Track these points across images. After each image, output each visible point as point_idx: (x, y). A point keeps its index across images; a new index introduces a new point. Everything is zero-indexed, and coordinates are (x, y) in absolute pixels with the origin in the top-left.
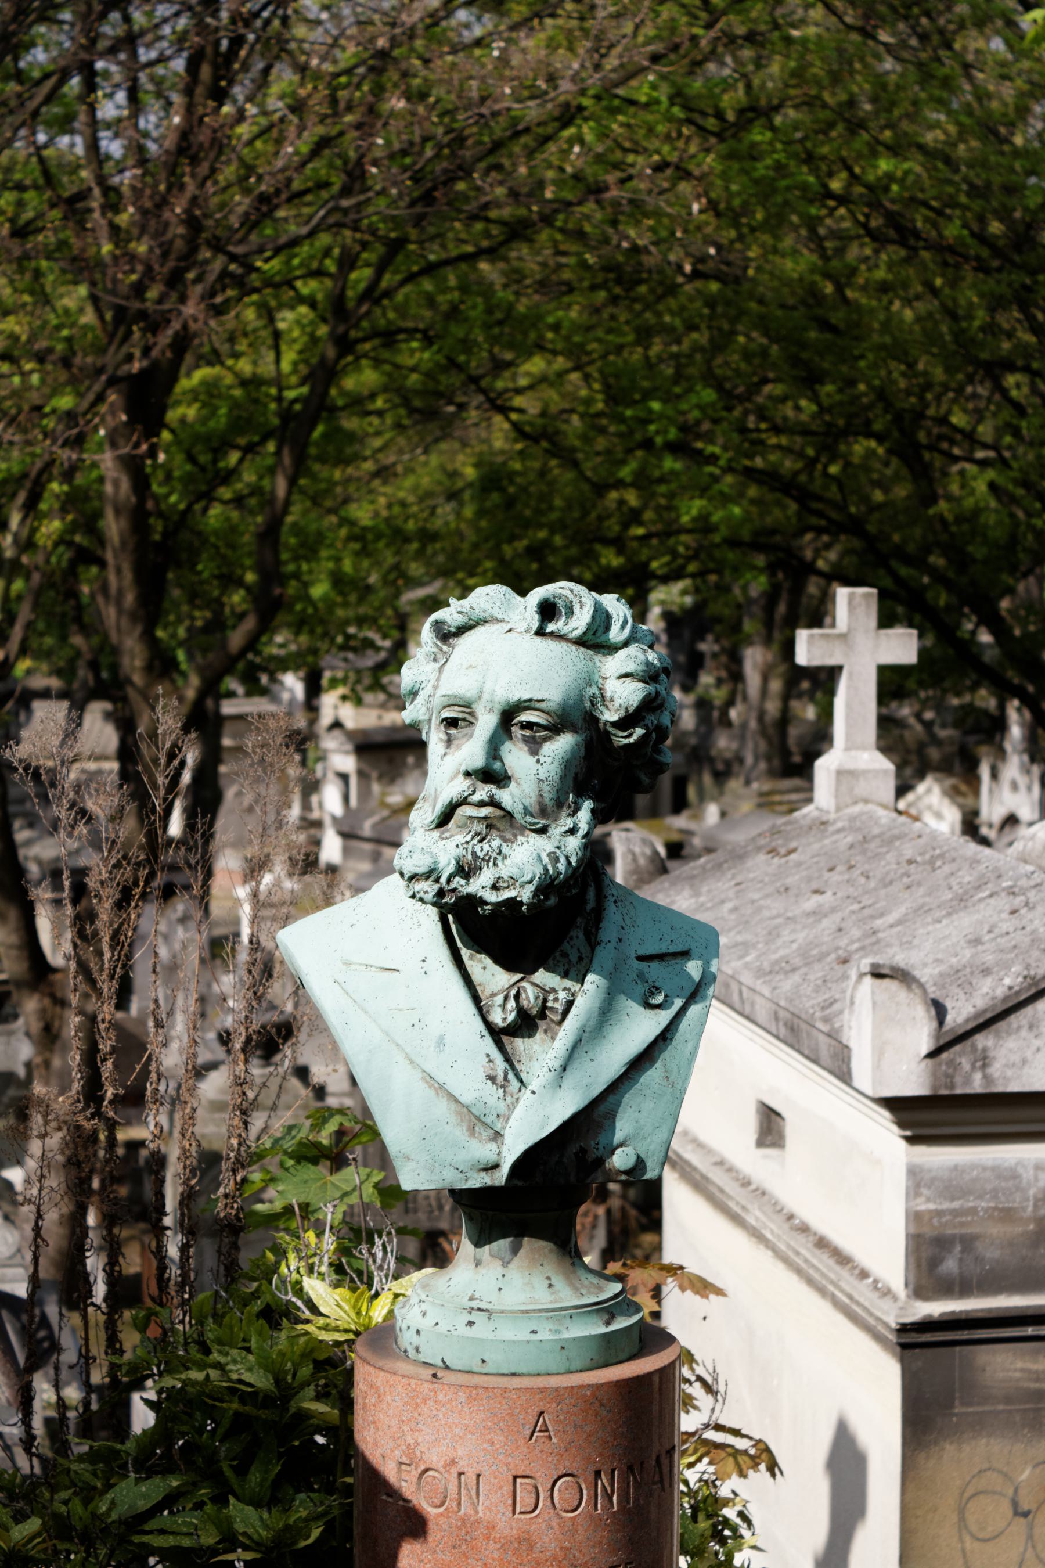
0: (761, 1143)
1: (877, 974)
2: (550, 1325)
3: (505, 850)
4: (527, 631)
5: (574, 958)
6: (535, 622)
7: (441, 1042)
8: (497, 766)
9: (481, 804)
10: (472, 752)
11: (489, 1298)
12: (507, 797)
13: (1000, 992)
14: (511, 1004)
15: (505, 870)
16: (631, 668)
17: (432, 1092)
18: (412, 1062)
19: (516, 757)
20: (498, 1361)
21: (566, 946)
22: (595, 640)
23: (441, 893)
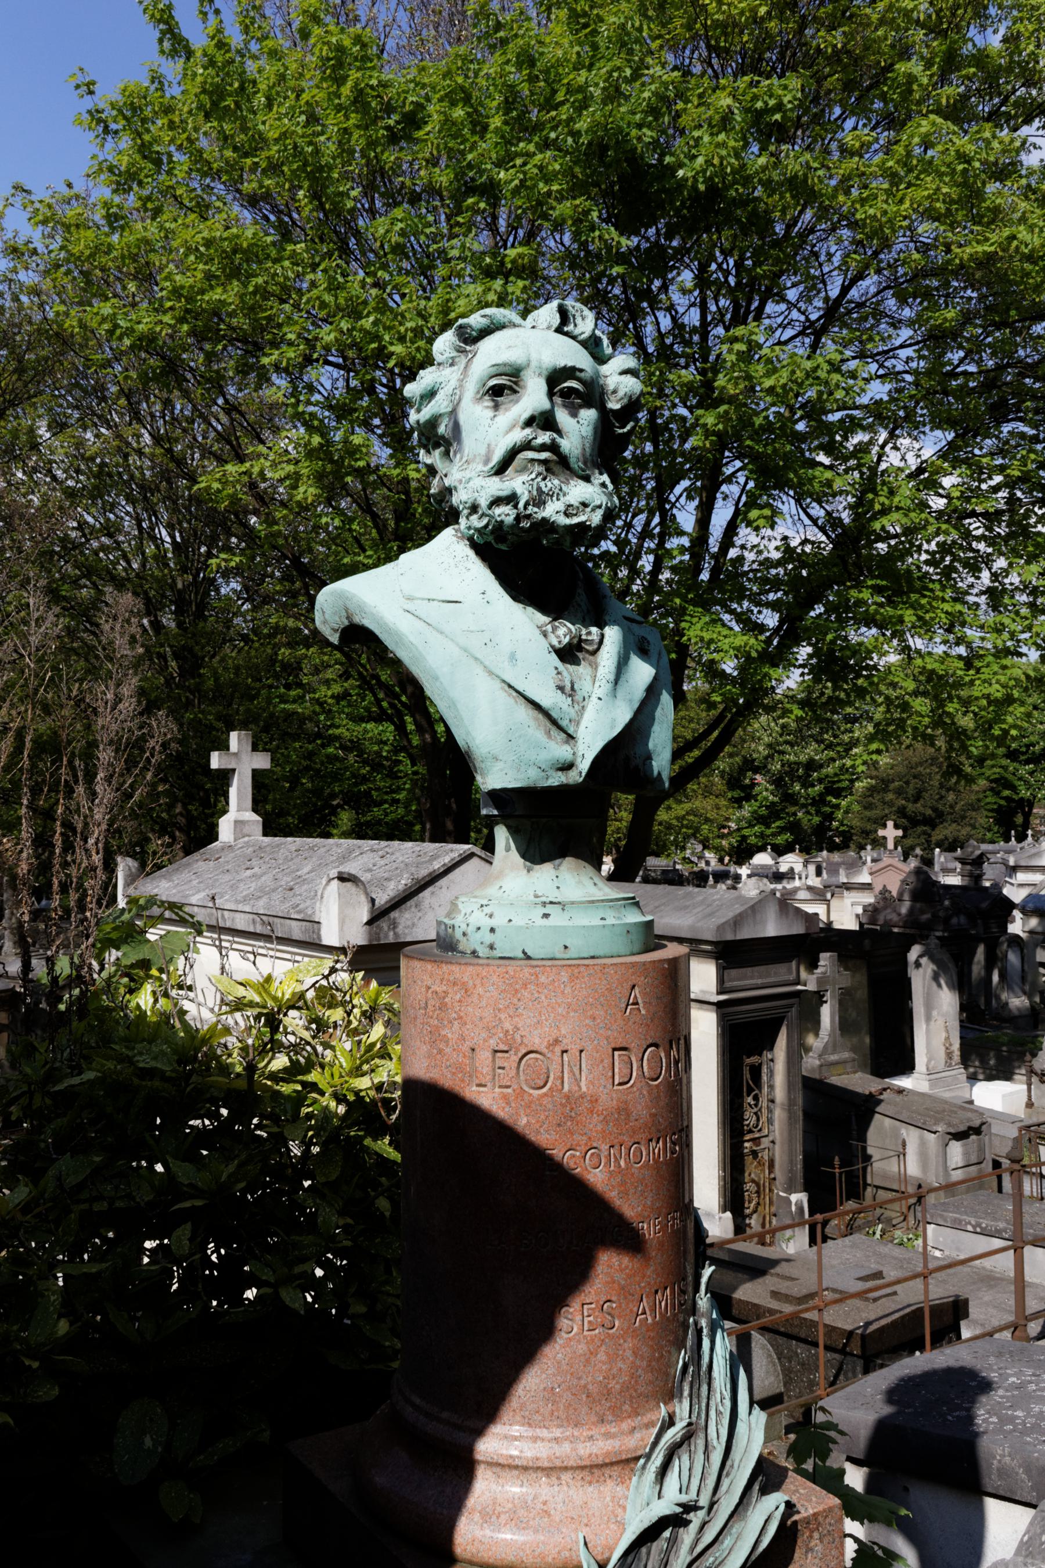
1: (342, 878)
6: (556, 320)
7: (513, 657)
9: (543, 448)
13: (401, 887)
18: (491, 673)
19: (562, 416)
20: (579, 947)
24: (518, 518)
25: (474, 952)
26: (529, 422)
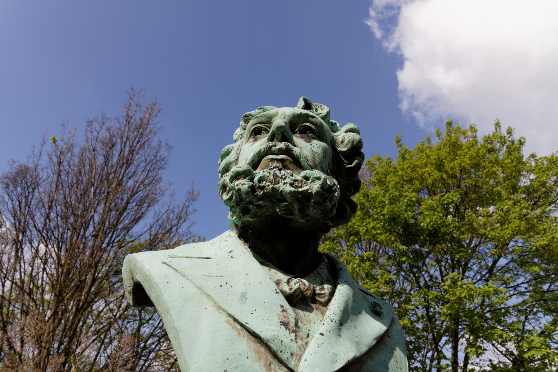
9: (280, 151)
17: (235, 333)
18: (219, 308)
24: (253, 189)
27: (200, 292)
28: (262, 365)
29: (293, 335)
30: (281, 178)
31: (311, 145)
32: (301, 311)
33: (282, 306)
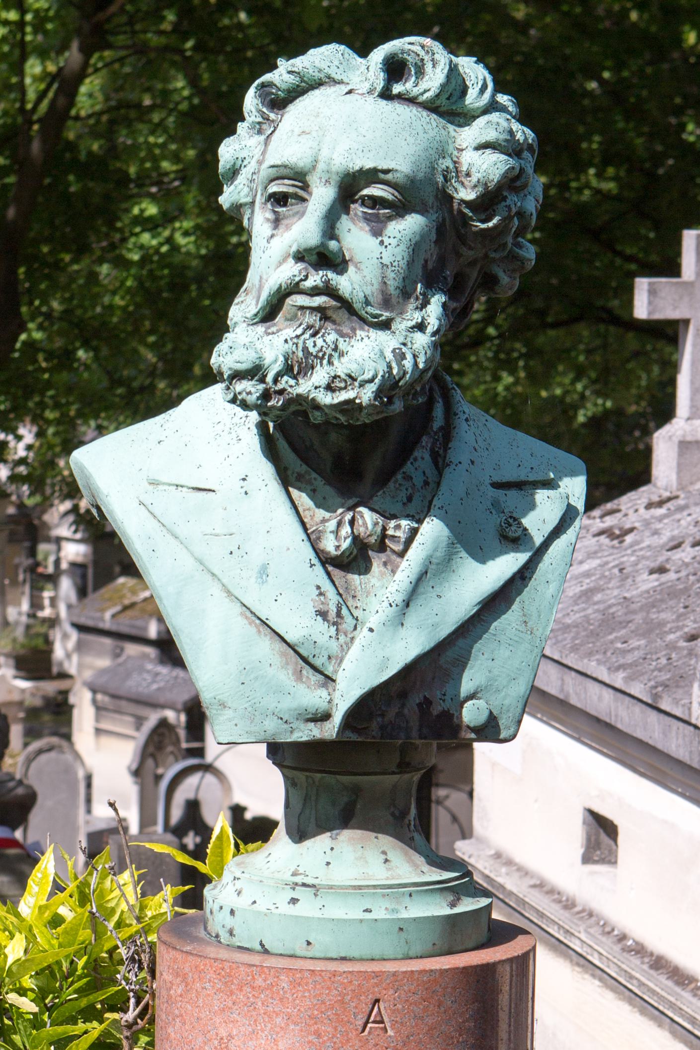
0: (587, 859)
2: (387, 903)
3: (342, 345)
4: (370, 92)
5: (418, 480)
7: (263, 572)
8: (333, 245)
9: (315, 292)
10: (305, 228)
11: (314, 872)
12: (345, 283)
14: (346, 530)
15: (341, 367)
16: (491, 135)
17: (253, 630)
18: (229, 593)
19: (355, 237)
20: (326, 943)
21: (408, 468)
22: (450, 107)
23: (266, 395)
25: (217, 936)
26: (299, 257)
27: (202, 567)
28: (290, 672)
29: (333, 629)
30: (316, 357)
31: (382, 243)
32: (356, 577)
33: (318, 587)
